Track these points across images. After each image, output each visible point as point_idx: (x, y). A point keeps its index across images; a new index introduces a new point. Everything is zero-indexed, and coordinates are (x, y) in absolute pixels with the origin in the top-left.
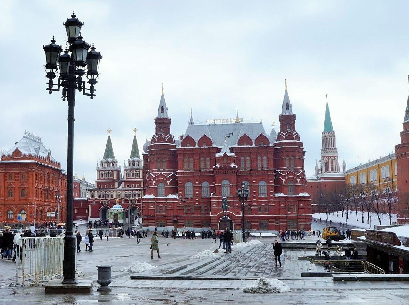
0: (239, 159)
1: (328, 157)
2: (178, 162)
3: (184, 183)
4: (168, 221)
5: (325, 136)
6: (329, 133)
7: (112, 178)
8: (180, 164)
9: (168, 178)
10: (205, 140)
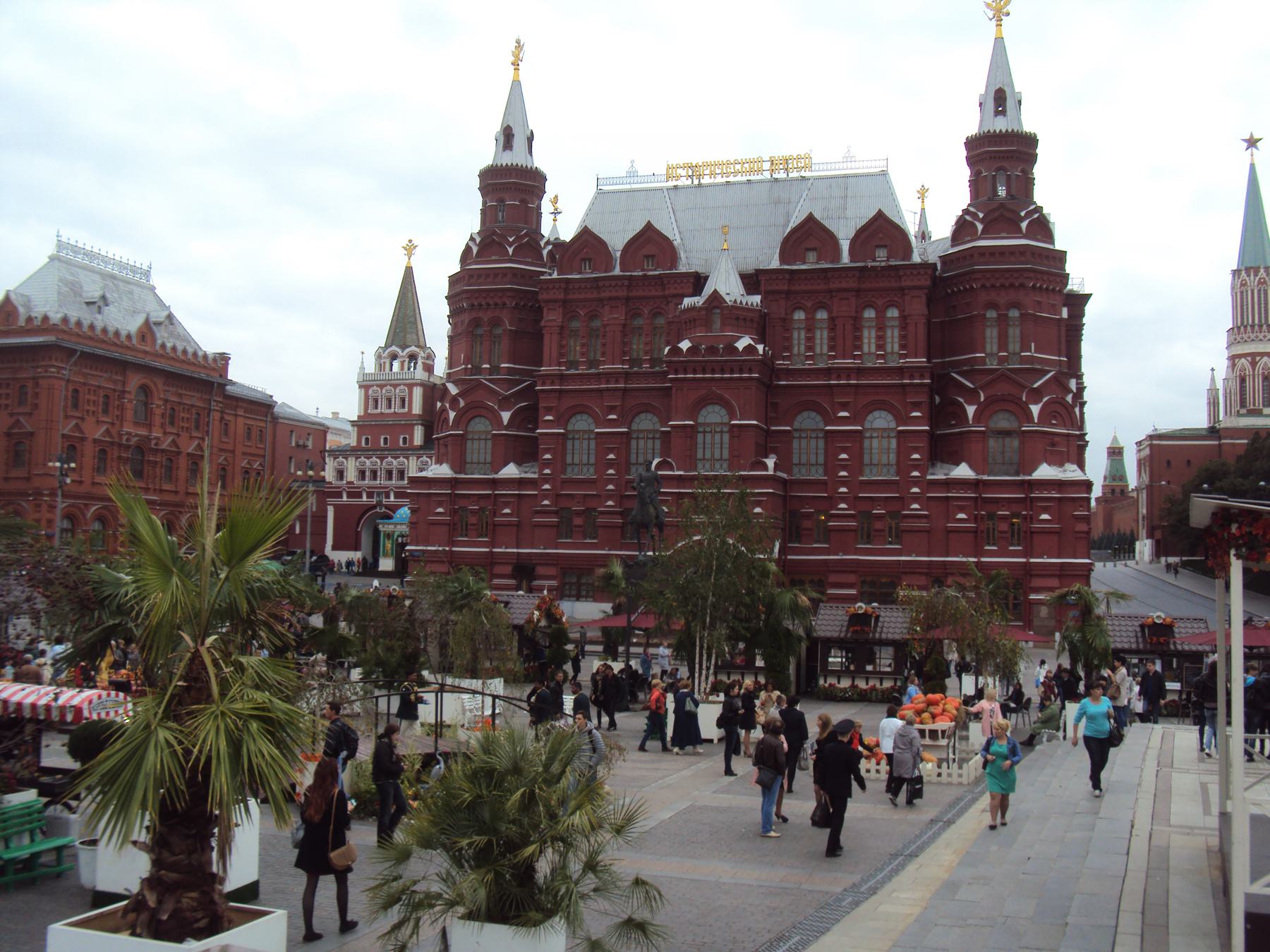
0: (786, 323)
1: (1253, 357)
2: (541, 336)
3: (561, 420)
4: (499, 570)
5: (1242, 285)
6: (1256, 275)
7: (406, 410)
8: (550, 344)
9: (506, 398)
10: (650, 243)
